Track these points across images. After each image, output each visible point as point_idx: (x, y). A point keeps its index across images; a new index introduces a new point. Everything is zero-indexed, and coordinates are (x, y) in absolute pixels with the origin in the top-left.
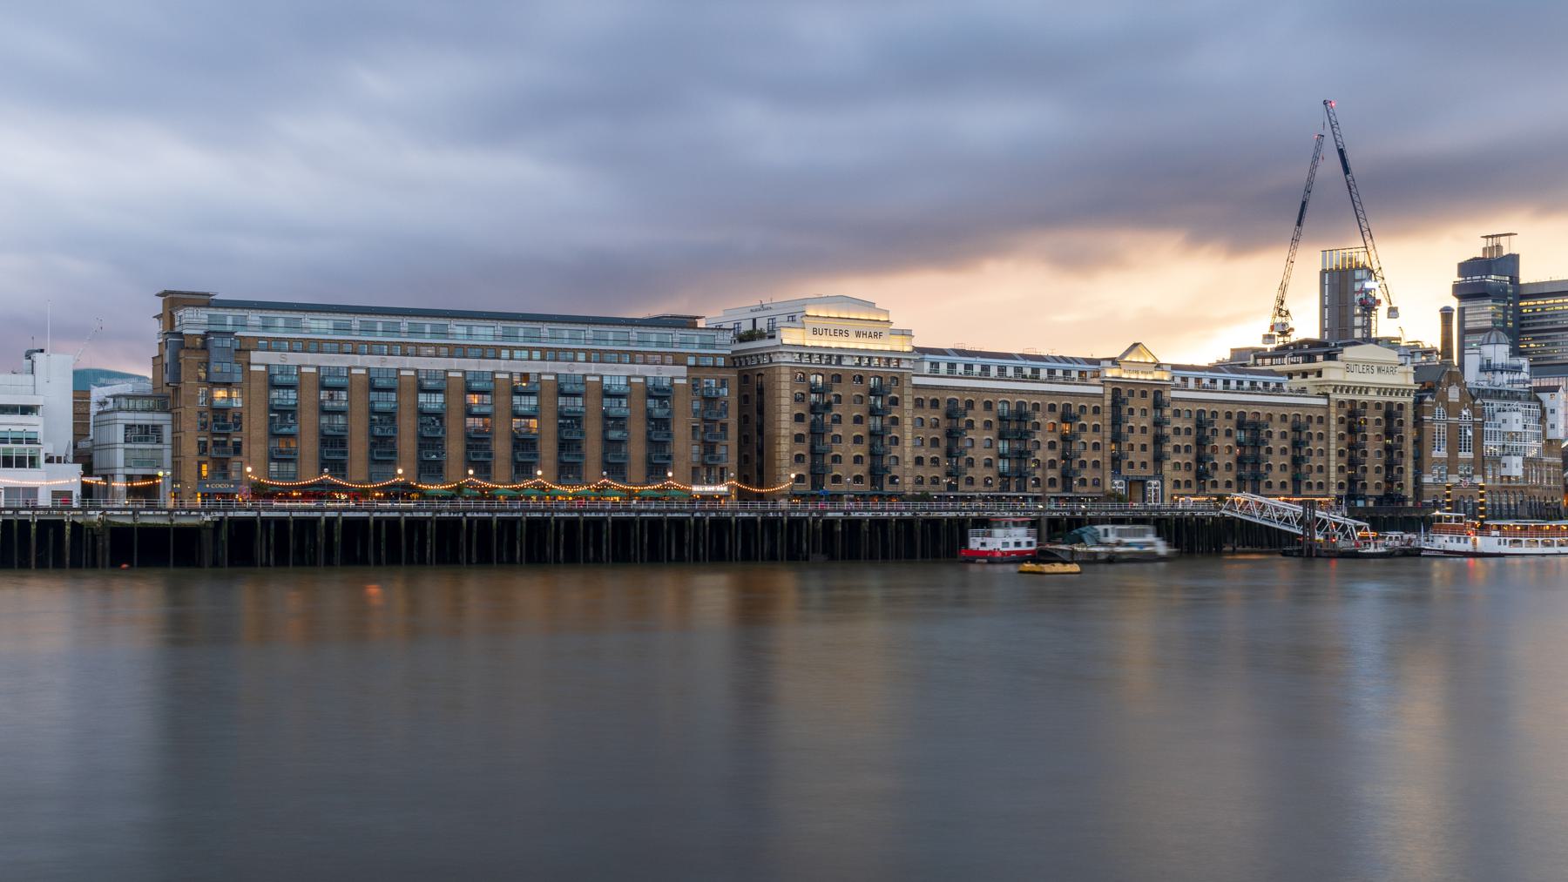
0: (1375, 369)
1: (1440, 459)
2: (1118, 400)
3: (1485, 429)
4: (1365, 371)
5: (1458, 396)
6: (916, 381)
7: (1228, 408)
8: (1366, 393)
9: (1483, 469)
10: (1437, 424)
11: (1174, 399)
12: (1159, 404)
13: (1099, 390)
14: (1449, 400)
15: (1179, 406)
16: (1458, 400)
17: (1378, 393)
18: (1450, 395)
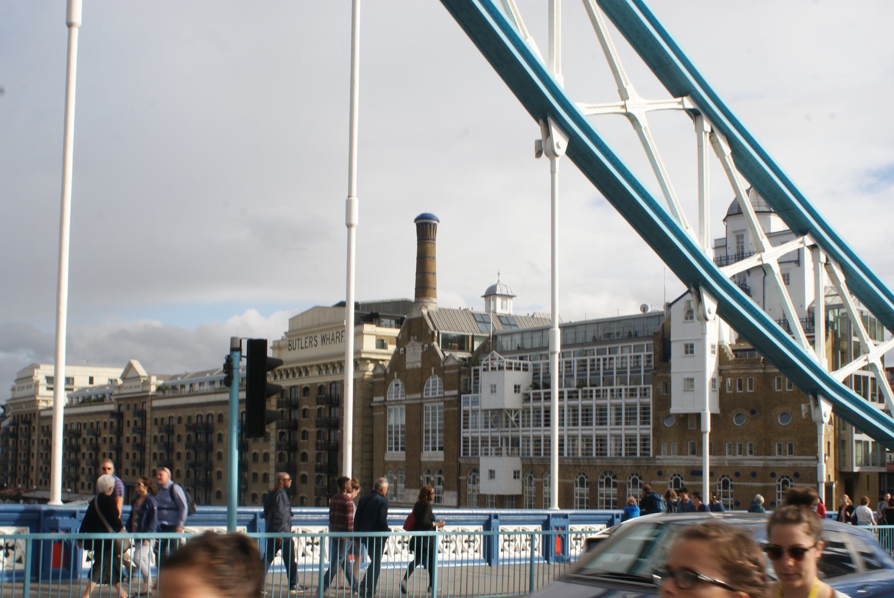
0: (319, 339)
1: (395, 463)
2: (118, 415)
3: (463, 408)
4: (307, 345)
5: (419, 358)
6: (43, 414)
7: (188, 412)
8: (307, 372)
9: (459, 481)
10: (430, 405)
11: (154, 409)
12: (142, 414)
13: (112, 407)
14: (407, 367)
15: (158, 415)
16: (419, 365)
17: (320, 370)
18: (408, 360)
